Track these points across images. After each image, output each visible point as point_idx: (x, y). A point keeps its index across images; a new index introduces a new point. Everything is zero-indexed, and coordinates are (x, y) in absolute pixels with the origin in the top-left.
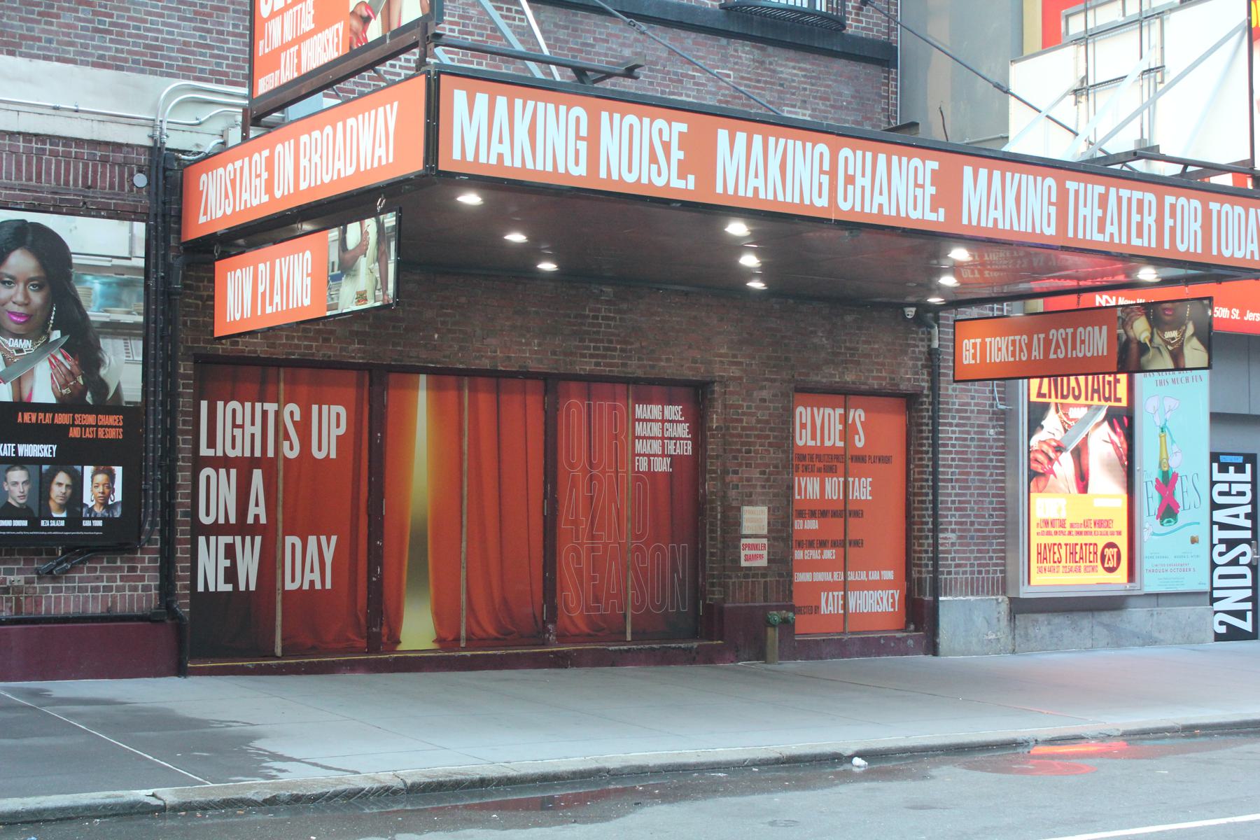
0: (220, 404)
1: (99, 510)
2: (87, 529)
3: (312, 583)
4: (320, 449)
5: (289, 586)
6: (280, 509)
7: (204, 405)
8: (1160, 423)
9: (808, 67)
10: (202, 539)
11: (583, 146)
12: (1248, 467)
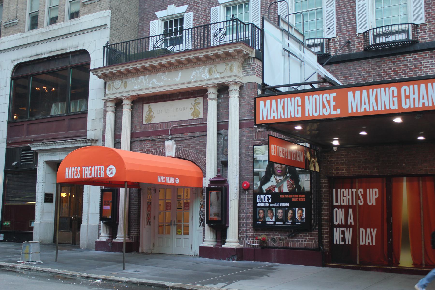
0: (339, 190)
1: (299, 220)
2: (297, 225)
3: (369, 243)
4: (370, 202)
5: (361, 243)
6: (357, 221)
7: (334, 190)
10: (335, 229)
11: (300, 108)
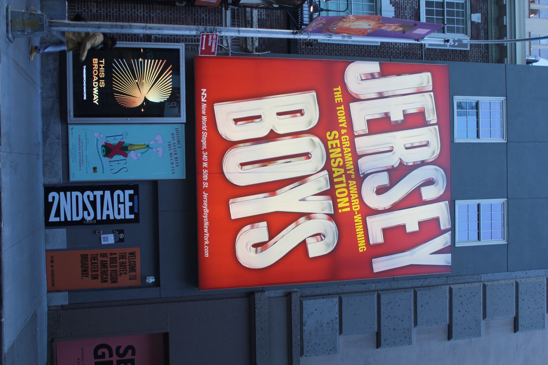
8: (152, 143)
9: (282, 18)
12: (132, 216)
